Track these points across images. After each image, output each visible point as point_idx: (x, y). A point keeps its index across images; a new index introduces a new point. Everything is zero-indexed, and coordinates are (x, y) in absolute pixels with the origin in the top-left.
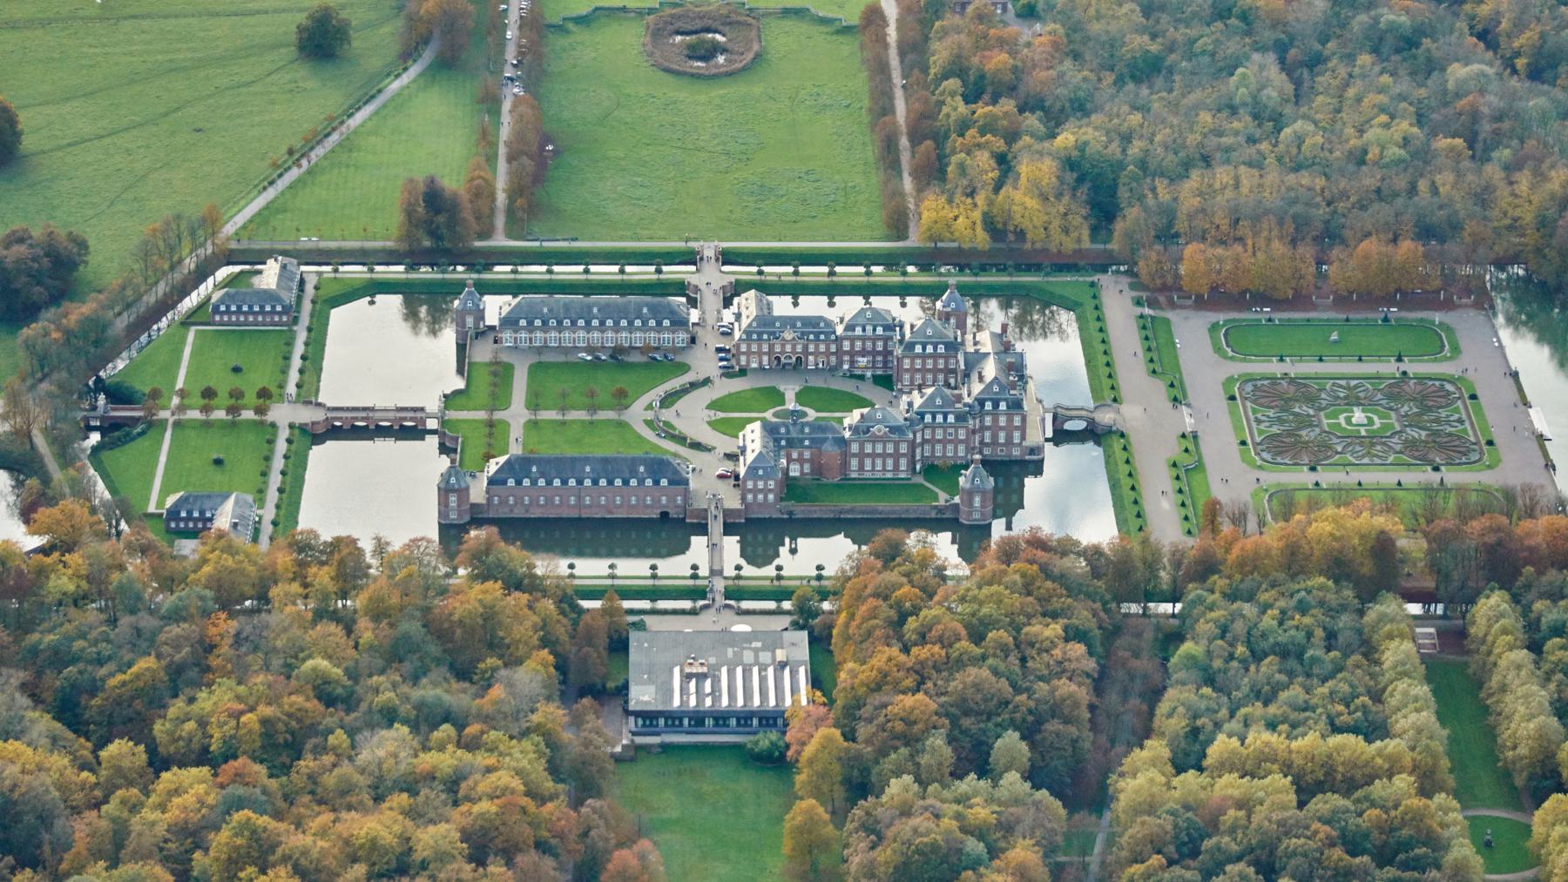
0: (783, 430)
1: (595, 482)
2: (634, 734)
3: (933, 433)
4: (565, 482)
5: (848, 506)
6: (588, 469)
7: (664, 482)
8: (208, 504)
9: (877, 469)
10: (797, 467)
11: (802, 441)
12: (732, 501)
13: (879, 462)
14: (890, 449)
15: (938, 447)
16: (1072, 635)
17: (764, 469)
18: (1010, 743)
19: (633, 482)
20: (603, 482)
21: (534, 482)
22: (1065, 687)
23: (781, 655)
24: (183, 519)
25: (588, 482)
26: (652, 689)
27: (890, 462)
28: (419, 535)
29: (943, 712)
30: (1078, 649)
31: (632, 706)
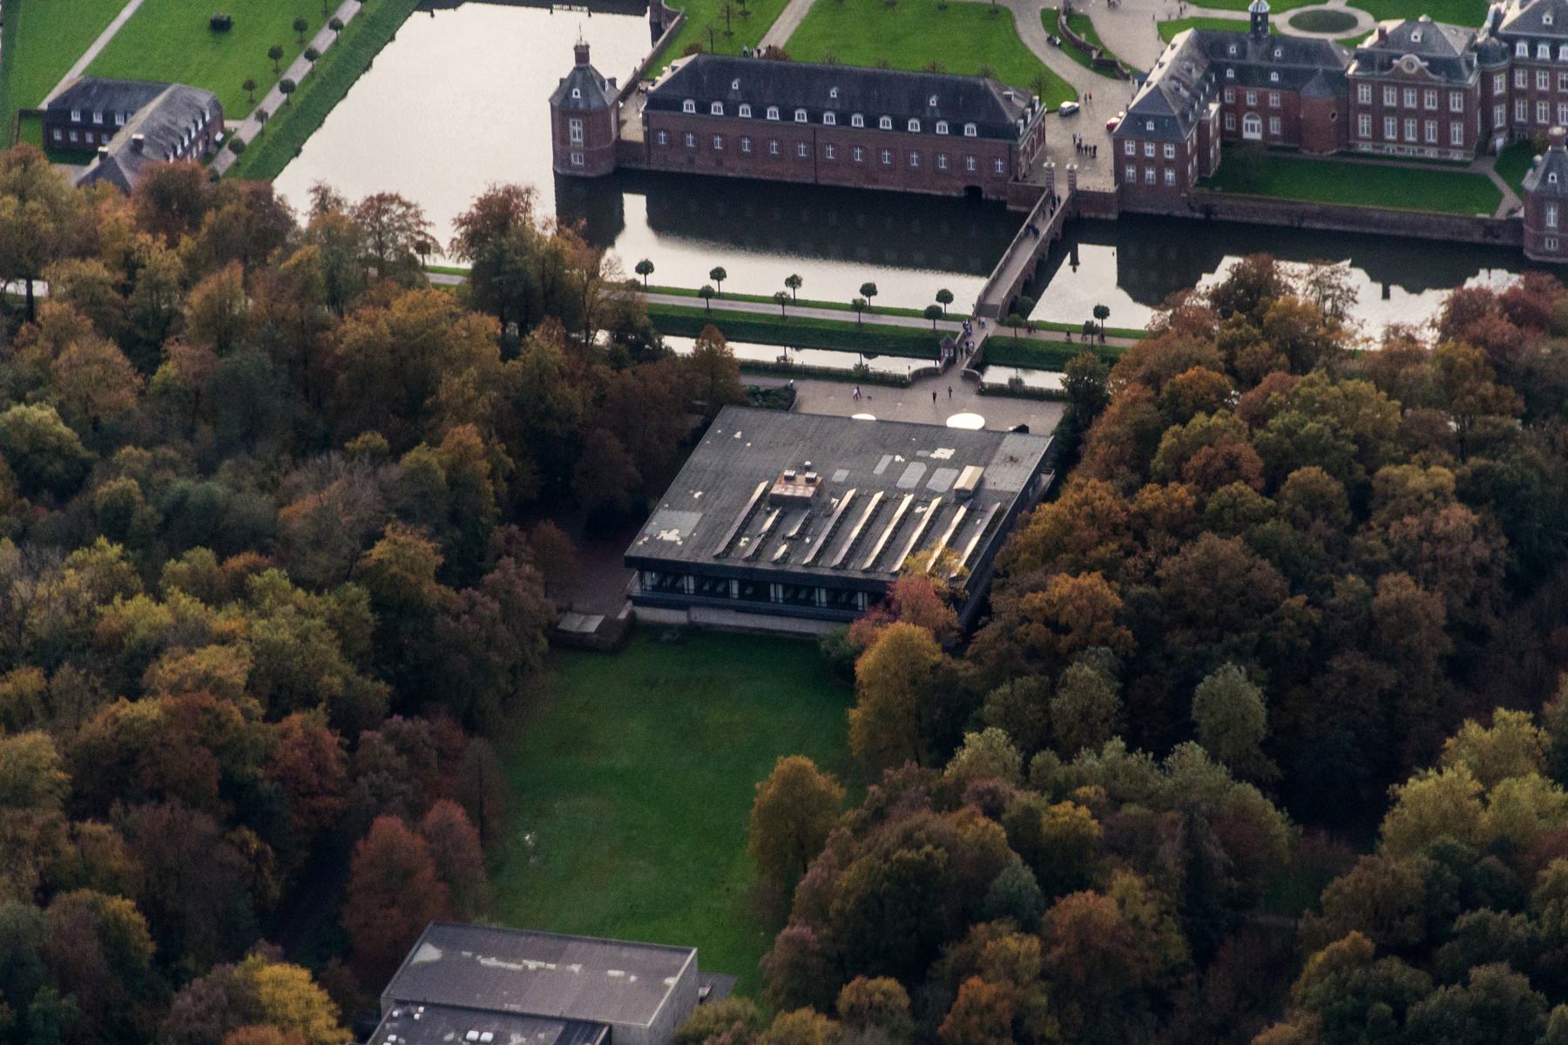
0: (1233, 50)
1: (844, 119)
2: (639, 602)
3: (1532, 78)
4: (787, 115)
5: (1317, 204)
6: (834, 93)
7: (970, 130)
8: (122, 102)
9: (1404, 139)
10: (1257, 122)
11: (1265, 73)
12: (1100, 180)
13: (1410, 125)
14: (1431, 102)
15: (1542, 107)
16: (1468, 494)
17: (1159, 122)
18: (1234, 687)
19: (914, 125)
20: (857, 120)
21: (731, 110)
22: (1398, 587)
23: (968, 478)
24: (75, 126)
25: (829, 118)
26: (693, 518)
27: (1431, 126)
28: (389, 190)
29: (1136, 615)
30: (1458, 515)
31: (640, 546)
